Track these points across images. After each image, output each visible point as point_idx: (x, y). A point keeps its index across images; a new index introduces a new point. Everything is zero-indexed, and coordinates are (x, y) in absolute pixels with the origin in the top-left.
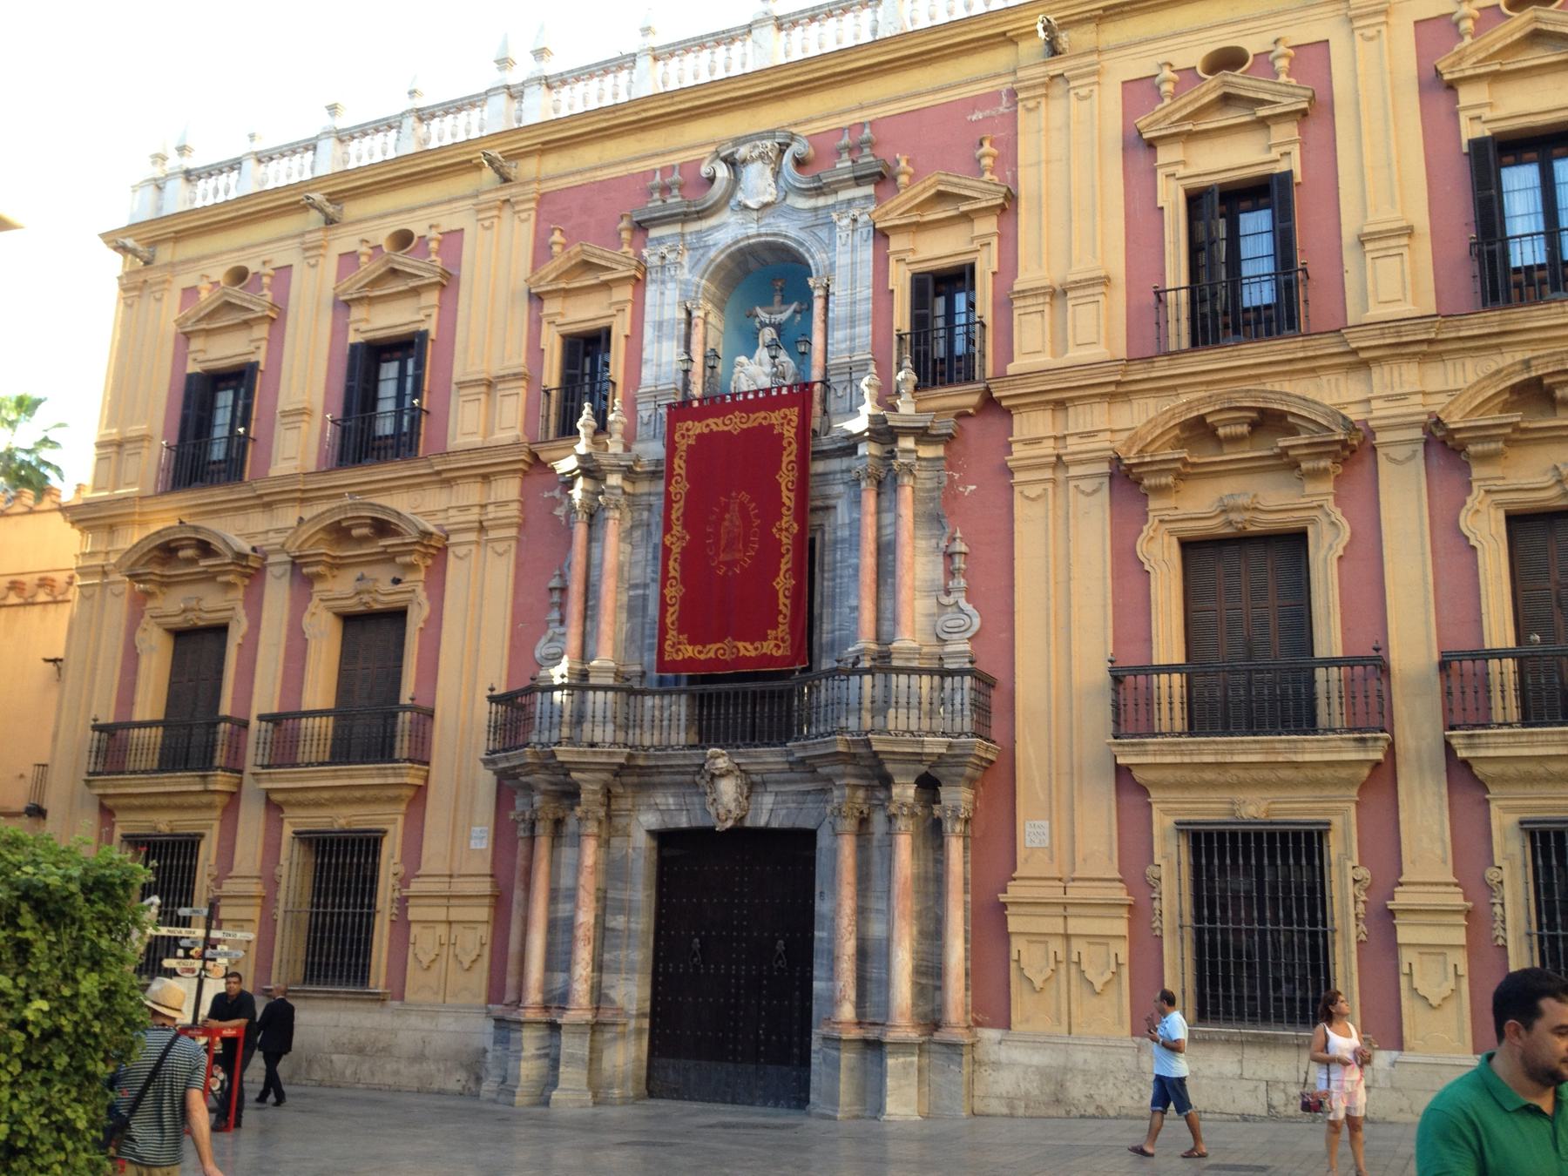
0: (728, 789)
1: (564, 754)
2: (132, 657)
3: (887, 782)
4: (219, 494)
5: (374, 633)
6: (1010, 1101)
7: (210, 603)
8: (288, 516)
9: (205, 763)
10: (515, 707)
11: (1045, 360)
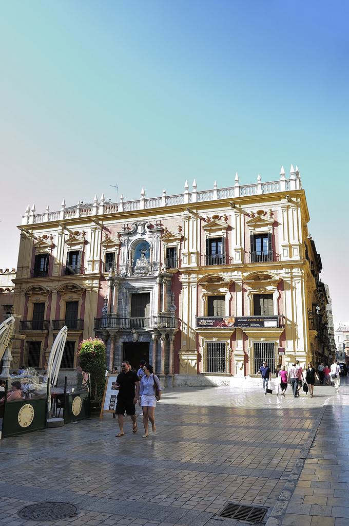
0: (135, 335)
1: (107, 329)
2: (26, 309)
3: (161, 335)
4: (43, 279)
5: (72, 306)
6: (179, 385)
7: (41, 299)
8: (56, 284)
9: (41, 329)
10: (98, 321)
11: (187, 266)
